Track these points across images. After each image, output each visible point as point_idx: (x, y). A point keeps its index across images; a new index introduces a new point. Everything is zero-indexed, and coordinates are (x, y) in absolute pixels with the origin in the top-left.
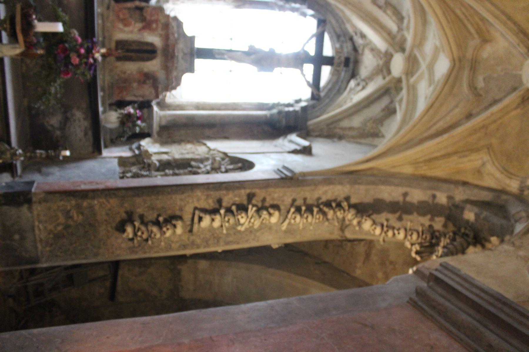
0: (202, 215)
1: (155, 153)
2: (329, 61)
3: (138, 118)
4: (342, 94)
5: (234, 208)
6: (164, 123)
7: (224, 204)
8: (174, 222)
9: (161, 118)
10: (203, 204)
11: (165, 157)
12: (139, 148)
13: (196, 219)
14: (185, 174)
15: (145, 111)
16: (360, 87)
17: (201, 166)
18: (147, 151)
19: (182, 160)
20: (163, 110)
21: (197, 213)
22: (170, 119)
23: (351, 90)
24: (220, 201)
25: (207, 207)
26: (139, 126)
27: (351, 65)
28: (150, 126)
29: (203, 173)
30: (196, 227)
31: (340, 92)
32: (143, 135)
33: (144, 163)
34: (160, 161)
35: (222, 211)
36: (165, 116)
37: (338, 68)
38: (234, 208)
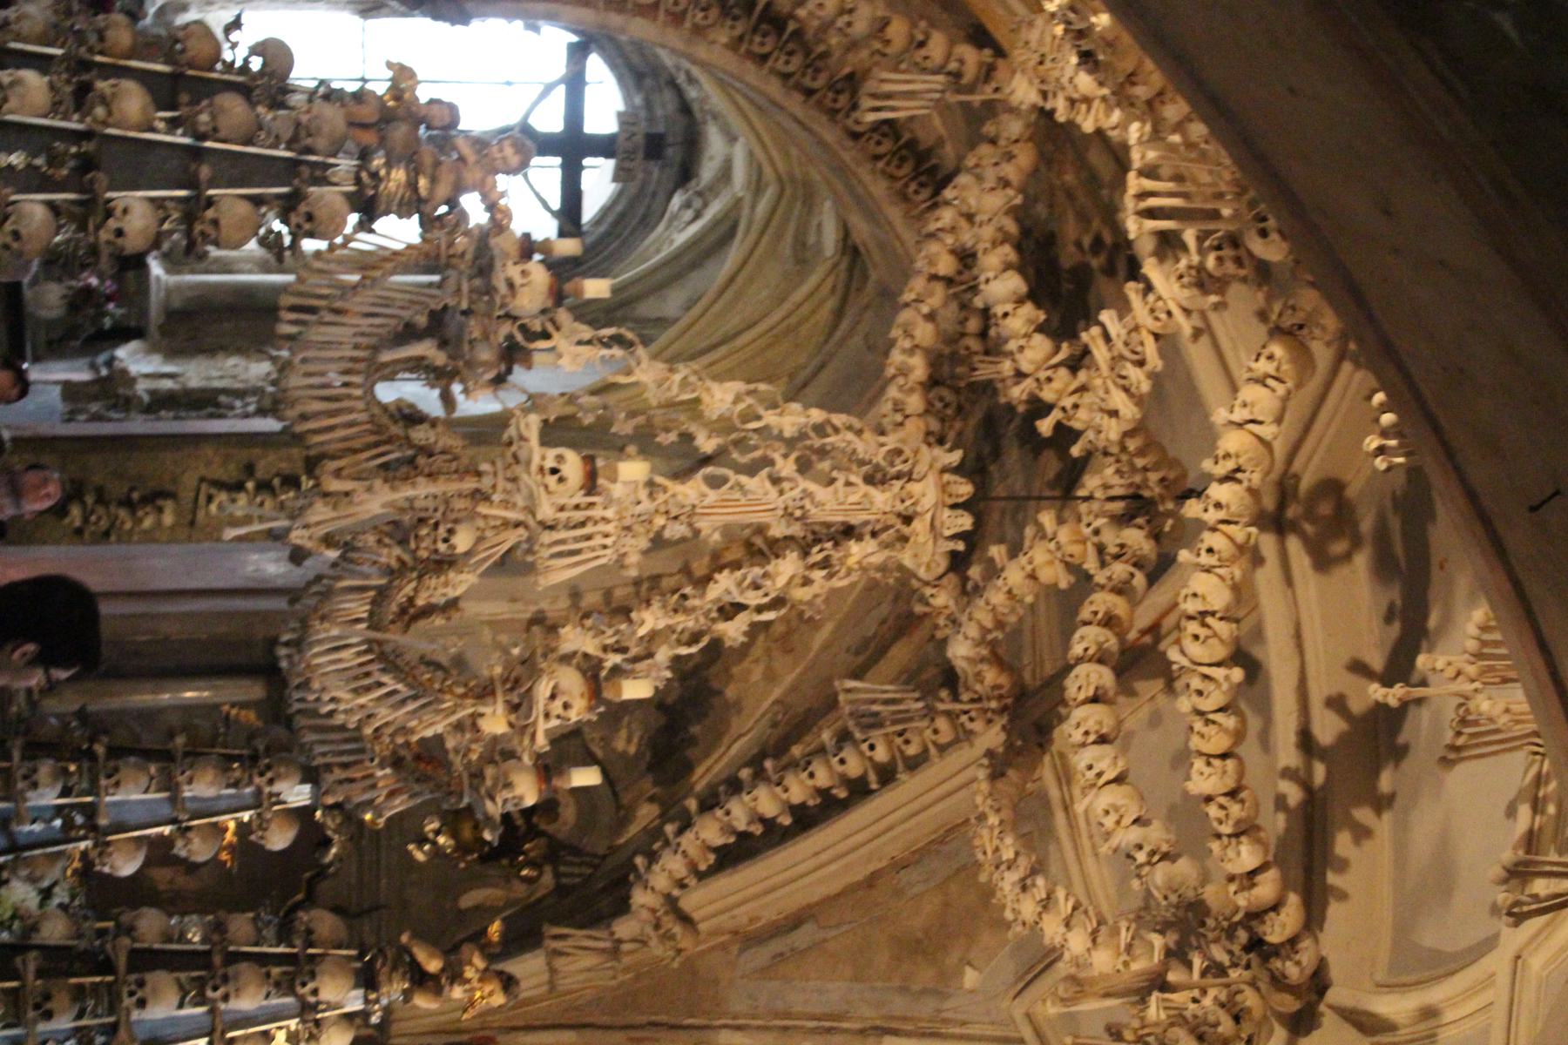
0: (213, 491)
1: (147, 376)
2: (604, 146)
3: (109, 298)
4: (654, 228)
5: (276, 482)
6: (177, 303)
7: (260, 474)
8: (160, 502)
9: (169, 291)
10: (218, 473)
11: (168, 384)
12: (110, 363)
13: (202, 499)
14: (199, 418)
15: (130, 275)
16: (689, 214)
17: (238, 403)
18: (124, 372)
19: (203, 391)
20: (179, 272)
21: (204, 487)
22: (190, 294)
23: (675, 217)
24: (250, 469)
25: (225, 478)
26: (112, 316)
27: (673, 153)
28: (144, 313)
29: (235, 416)
30: (201, 515)
31: (647, 222)
32: (123, 334)
33: (118, 396)
34: (152, 393)
35: (250, 485)
36: (179, 288)
37: (627, 164)
38: (276, 482)
